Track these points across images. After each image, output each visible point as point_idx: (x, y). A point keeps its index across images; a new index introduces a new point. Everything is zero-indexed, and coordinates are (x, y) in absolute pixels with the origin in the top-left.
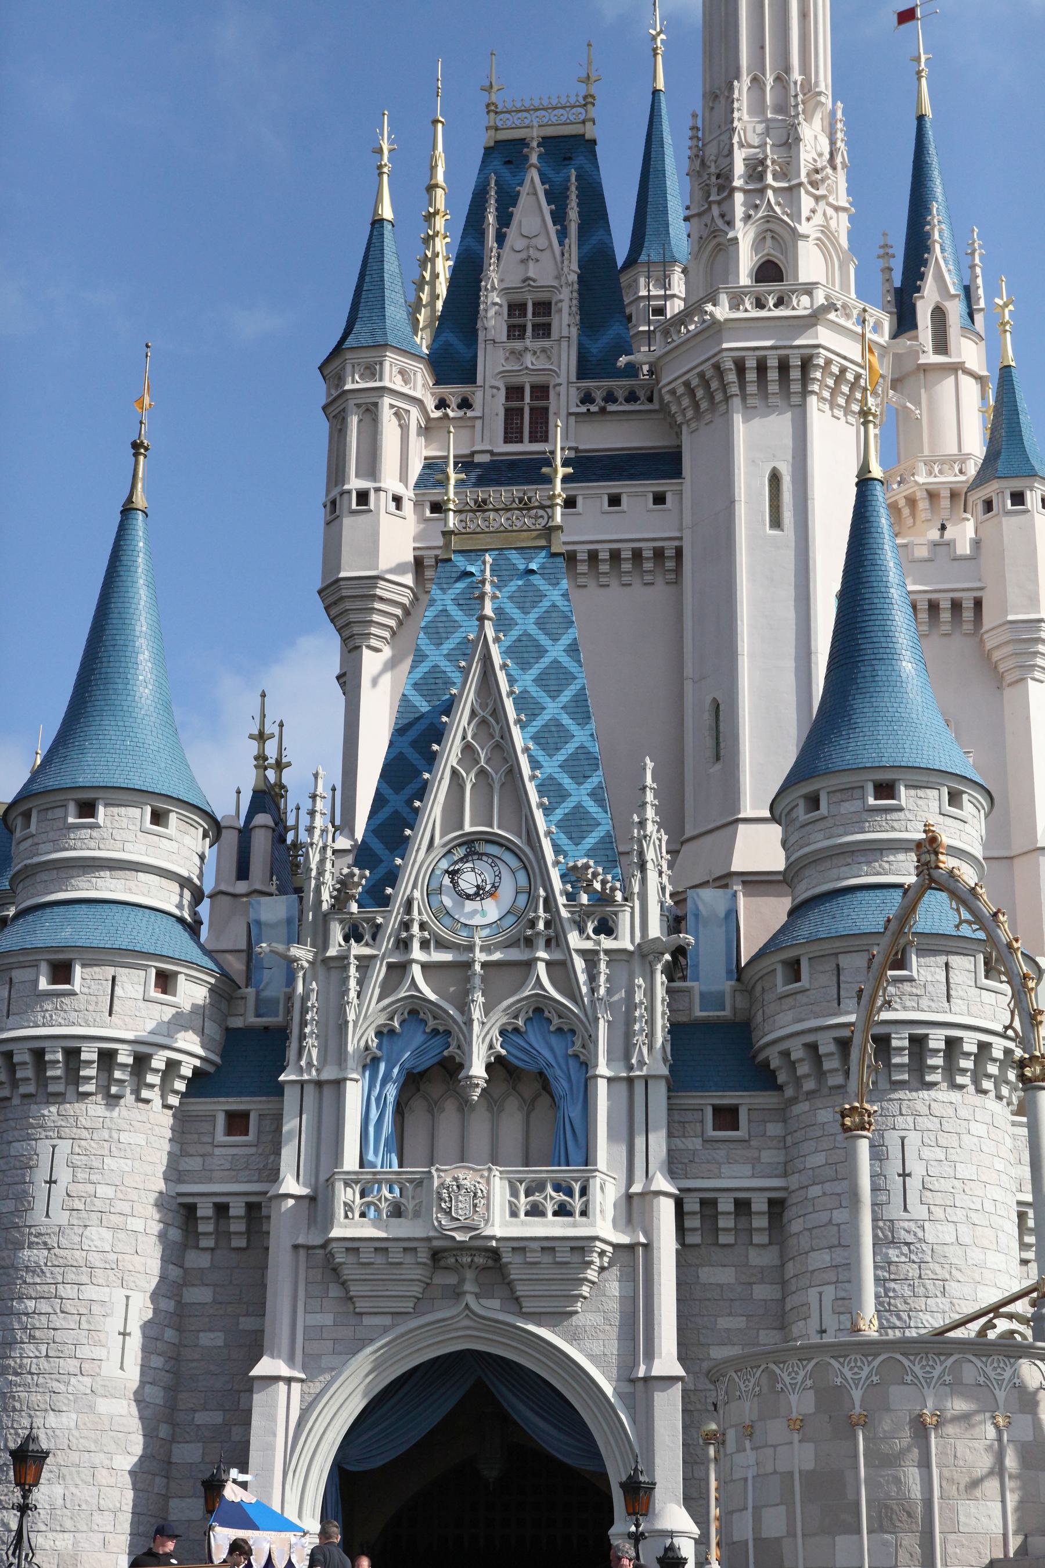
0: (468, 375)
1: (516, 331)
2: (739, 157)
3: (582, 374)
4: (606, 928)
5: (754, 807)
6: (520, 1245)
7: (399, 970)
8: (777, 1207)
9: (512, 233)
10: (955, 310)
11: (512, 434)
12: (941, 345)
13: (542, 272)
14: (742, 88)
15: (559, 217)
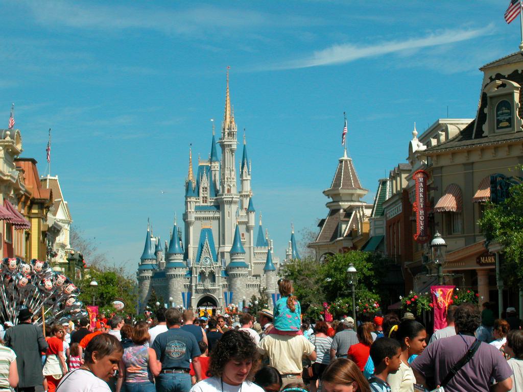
0: (199, 196)
1: (203, 191)
2: (226, 177)
3: (210, 196)
4: (217, 264)
5: (228, 244)
6: (211, 289)
7: (201, 268)
8: (229, 285)
9: (203, 180)
10: (247, 172)
11: (203, 202)
12: (246, 177)
13: (206, 186)
14: (226, 169)
15: (208, 178)
